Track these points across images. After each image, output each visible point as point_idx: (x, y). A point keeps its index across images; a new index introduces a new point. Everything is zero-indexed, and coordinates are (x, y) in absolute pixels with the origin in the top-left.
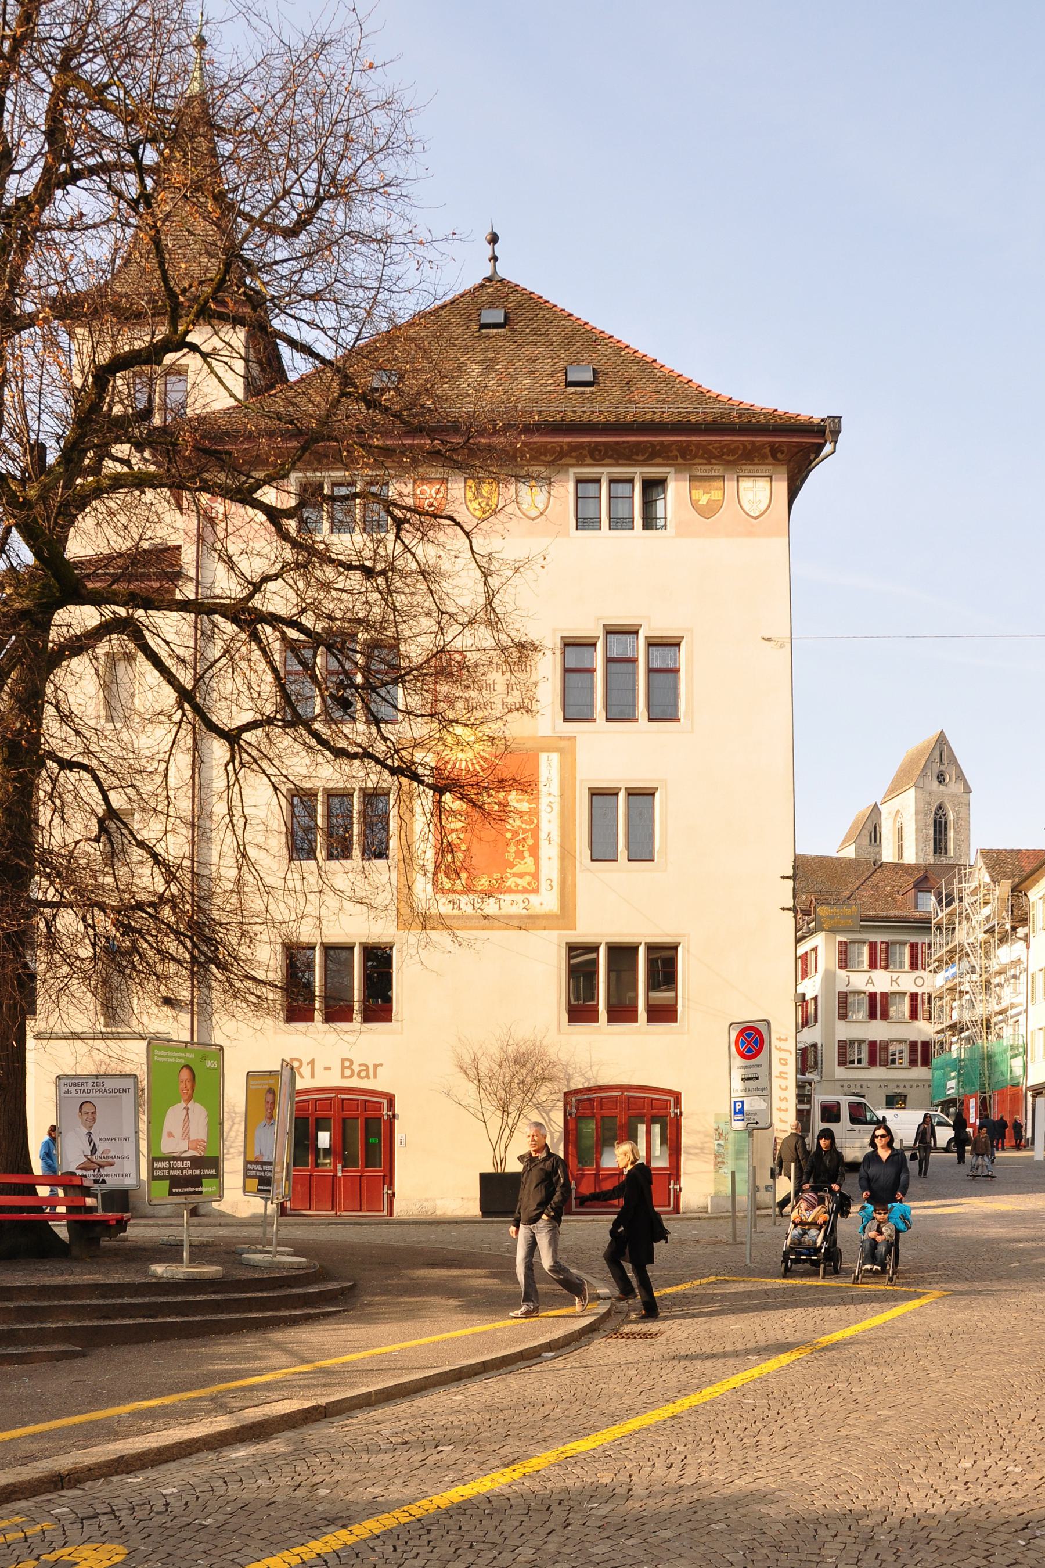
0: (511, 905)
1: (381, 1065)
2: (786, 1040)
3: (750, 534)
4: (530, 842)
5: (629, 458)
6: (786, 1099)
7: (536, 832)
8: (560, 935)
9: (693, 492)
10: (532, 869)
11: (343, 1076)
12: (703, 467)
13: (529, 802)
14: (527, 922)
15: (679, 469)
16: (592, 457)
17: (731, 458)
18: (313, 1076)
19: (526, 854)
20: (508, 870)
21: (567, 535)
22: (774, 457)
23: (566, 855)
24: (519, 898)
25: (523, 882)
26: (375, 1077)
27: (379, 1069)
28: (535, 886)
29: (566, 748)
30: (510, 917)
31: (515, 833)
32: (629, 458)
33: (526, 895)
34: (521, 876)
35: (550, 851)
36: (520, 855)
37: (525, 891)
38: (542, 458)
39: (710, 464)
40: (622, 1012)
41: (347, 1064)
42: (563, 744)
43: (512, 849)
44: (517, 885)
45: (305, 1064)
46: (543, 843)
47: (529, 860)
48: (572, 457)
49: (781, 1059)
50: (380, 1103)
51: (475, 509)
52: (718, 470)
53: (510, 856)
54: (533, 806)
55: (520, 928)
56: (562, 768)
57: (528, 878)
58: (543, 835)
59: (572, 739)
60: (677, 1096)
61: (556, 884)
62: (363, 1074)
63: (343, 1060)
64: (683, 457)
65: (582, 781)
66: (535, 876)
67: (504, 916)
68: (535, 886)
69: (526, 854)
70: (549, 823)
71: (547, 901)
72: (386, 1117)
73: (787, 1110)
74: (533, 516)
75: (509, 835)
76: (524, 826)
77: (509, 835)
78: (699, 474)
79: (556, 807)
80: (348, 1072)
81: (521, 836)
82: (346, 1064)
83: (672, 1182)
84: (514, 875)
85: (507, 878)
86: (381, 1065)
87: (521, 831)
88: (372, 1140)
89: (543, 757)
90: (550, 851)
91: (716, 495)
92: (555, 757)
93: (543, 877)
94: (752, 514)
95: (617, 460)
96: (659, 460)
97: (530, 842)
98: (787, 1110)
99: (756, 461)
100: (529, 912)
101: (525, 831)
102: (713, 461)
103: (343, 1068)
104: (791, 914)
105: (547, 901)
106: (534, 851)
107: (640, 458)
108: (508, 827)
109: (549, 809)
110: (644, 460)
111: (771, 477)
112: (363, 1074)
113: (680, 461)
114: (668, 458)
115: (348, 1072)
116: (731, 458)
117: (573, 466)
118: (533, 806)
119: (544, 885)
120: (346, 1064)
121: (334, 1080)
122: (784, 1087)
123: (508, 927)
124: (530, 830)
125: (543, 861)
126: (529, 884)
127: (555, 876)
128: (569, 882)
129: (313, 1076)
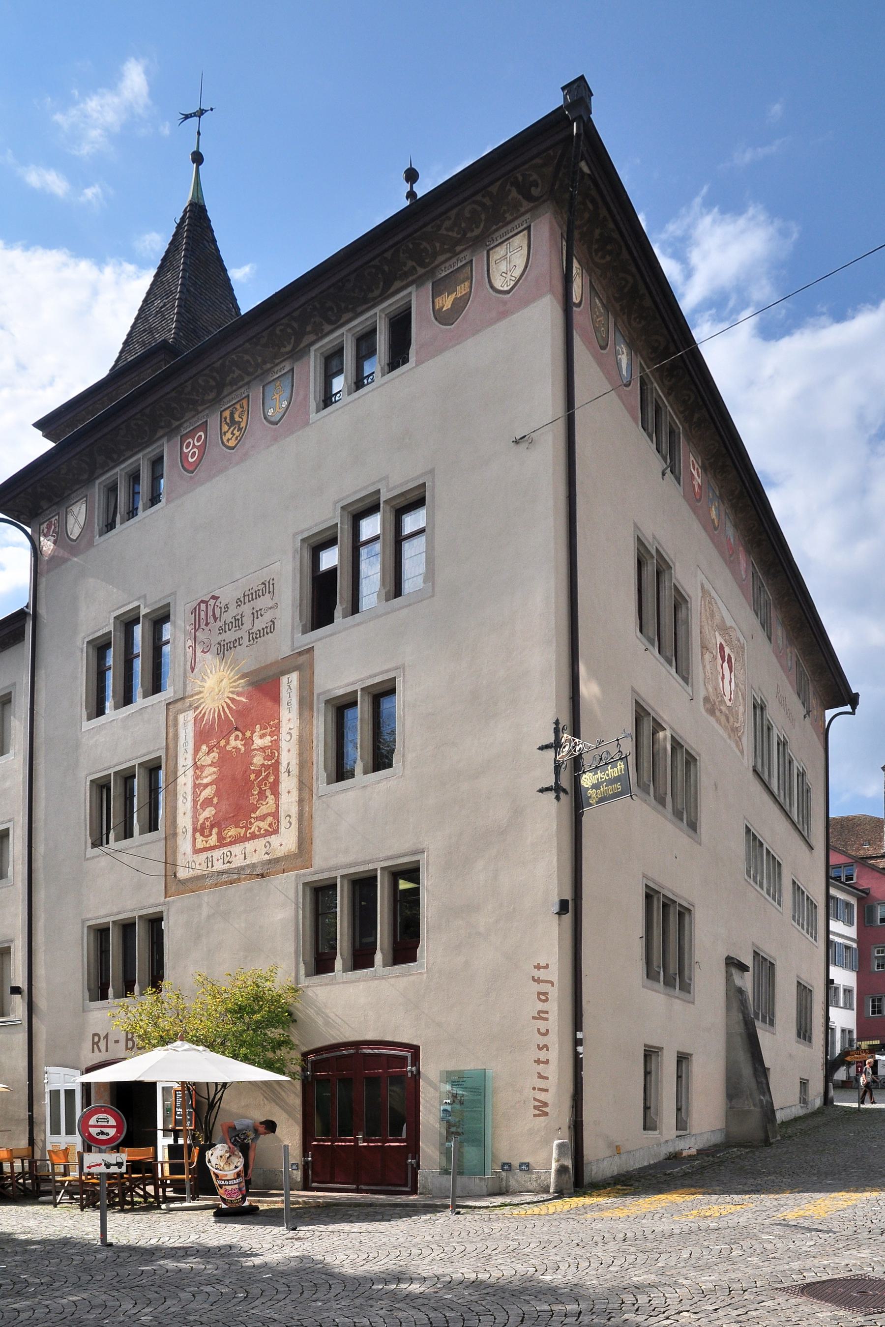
2: (547, 967)
3: (503, 315)
4: (271, 779)
6: (546, 1046)
9: (436, 300)
11: (127, 1049)
12: (447, 264)
15: (419, 282)
17: (477, 232)
19: (268, 793)
20: (253, 815)
21: (307, 423)
22: (529, 198)
23: (304, 785)
25: (264, 825)
29: (302, 662)
30: (254, 866)
31: (258, 773)
32: (365, 300)
35: (288, 784)
36: (262, 795)
37: (268, 833)
44: (260, 829)
46: (283, 776)
47: (271, 799)
48: (310, 333)
49: (539, 993)
51: (228, 440)
53: (253, 800)
54: (275, 737)
56: (301, 687)
57: (270, 819)
58: (283, 768)
60: (415, 1050)
61: (294, 820)
64: (422, 264)
65: (319, 695)
66: (275, 815)
67: (247, 865)
68: (275, 826)
69: (268, 793)
70: (288, 756)
73: (547, 1062)
75: (253, 777)
76: (266, 763)
77: (253, 777)
78: (443, 274)
79: (295, 734)
80: (130, 1044)
83: (410, 1155)
84: (257, 819)
89: (284, 680)
90: (288, 784)
91: (461, 290)
92: (294, 677)
93: (282, 815)
94: (506, 288)
96: (398, 284)
97: (271, 779)
98: (547, 1062)
99: (509, 217)
101: (267, 767)
102: (458, 248)
103: (127, 1040)
104: (552, 795)
105: (286, 841)
111: (528, 228)
113: (421, 271)
114: (406, 275)
115: (130, 1044)
116: (477, 232)
117: (313, 343)
118: (275, 737)
119: (284, 823)
122: (543, 1031)
123: (251, 876)
124: (270, 766)
126: (270, 825)
127: (294, 810)
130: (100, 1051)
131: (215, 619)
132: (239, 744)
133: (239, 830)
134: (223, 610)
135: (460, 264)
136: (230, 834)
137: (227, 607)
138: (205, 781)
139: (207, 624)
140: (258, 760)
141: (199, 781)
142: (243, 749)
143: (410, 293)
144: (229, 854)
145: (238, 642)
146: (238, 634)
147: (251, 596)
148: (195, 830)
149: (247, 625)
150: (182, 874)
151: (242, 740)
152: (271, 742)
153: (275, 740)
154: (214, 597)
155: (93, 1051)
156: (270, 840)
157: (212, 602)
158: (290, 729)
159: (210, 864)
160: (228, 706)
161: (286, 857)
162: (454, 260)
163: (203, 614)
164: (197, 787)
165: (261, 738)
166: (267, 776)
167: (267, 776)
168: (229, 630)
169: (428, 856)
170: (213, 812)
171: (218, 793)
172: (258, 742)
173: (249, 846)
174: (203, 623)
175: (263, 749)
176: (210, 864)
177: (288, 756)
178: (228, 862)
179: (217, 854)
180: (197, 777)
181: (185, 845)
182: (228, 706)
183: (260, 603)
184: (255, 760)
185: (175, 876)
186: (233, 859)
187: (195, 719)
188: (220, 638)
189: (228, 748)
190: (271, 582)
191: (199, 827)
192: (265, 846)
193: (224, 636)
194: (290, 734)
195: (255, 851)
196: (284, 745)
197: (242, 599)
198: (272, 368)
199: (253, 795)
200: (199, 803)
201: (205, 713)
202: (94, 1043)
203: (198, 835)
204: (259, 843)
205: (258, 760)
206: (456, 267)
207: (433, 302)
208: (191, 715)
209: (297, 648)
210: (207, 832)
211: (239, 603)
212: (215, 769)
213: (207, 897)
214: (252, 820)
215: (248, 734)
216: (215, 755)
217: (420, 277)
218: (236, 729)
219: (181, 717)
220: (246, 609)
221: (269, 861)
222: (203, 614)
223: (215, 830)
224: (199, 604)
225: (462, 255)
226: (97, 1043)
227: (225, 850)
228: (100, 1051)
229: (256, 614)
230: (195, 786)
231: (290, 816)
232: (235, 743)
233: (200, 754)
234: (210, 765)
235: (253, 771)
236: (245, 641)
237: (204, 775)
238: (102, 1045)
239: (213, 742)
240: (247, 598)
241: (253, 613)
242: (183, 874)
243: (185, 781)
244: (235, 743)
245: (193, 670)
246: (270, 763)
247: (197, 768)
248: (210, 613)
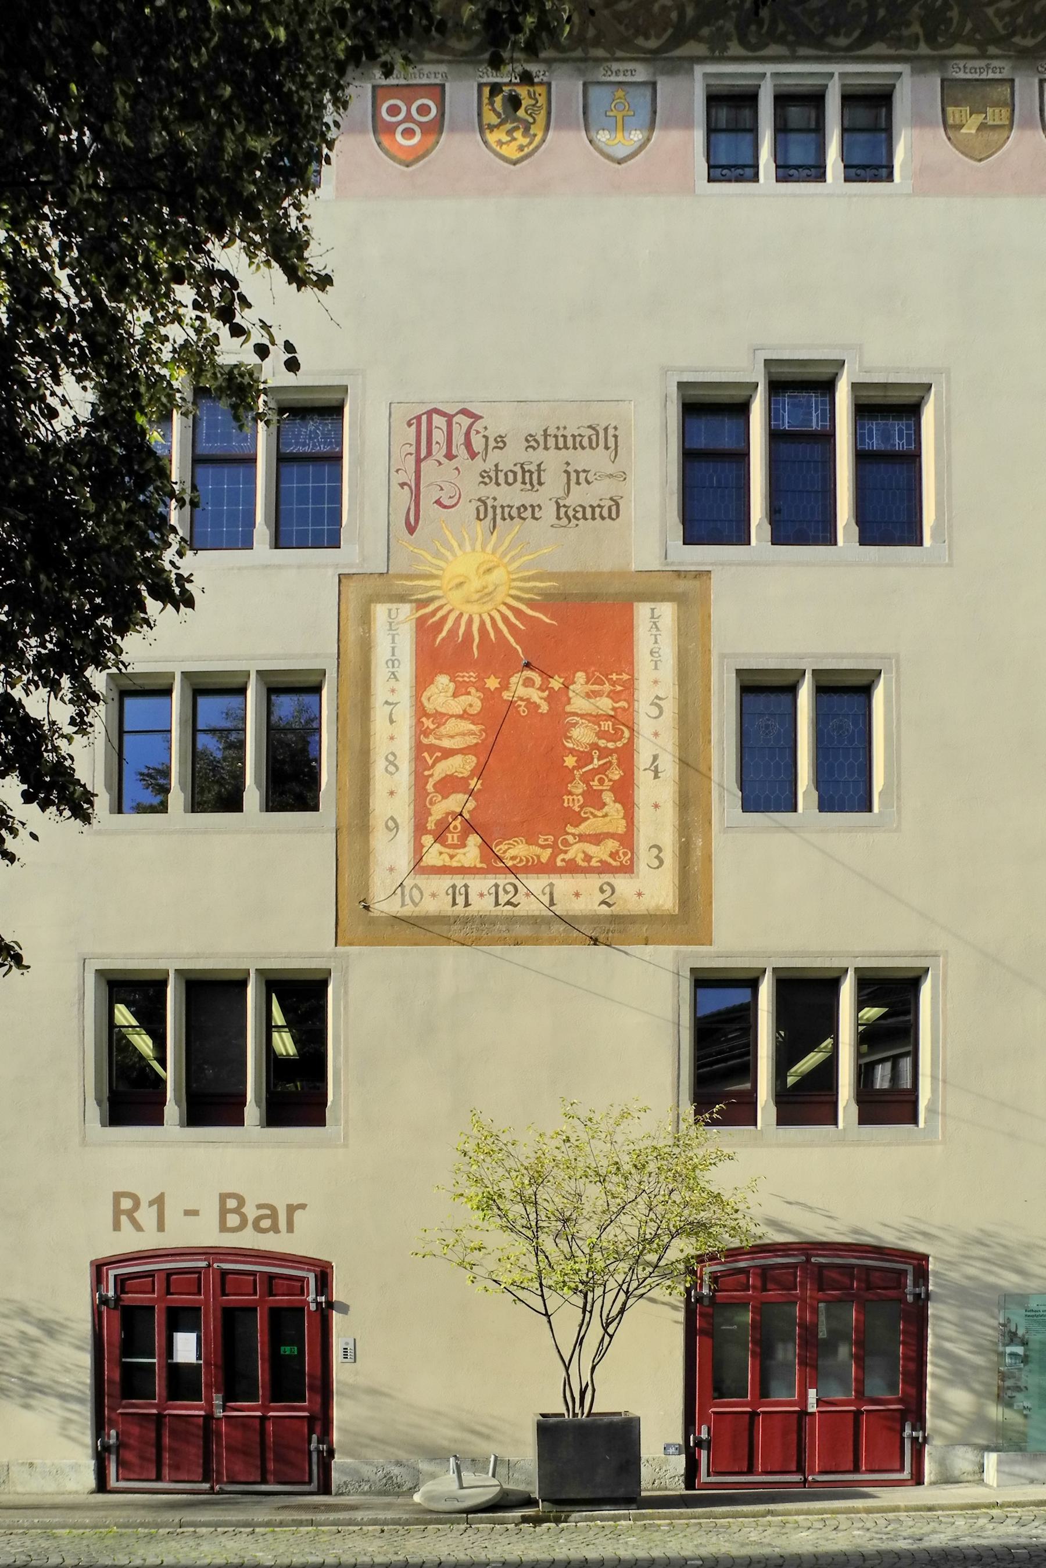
0: (577, 894)
1: (303, 1206)
4: (616, 774)
5: (818, 42)
7: (627, 756)
8: (677, 953)
9: (950, 110)
10: (621, 827)
11: (223, 1228)
12: (970, 64)
13: (614, 696)
14: (607, 931)
15: (920, 65)
16: (743, 42)
18: (161, 1227)
19: (608, 797)
20: (570, 829)
24: (594, 881)
25: (600, 853)
26: (290, 1228)
27: (298, 1215)
28: (625, 860)
29: (688, 593)
31: (584, 758)
33: (607, 878)
34: (597, 839)
35: (656, 794)
36: (594, 799)
37: (605, 868)
38: (640, 41)
39: (983, 56)
40: (806, 1102)
41: (232, 1204)
42: (681, 585)
43: (578, 788)
44: (588, 858)
45: (144, 1204)
46: (643, 779)
47: (614, 809)
50: (301, 1279)
52: (1000, 68)
53: (574, 801)
55: (595, 941)
57: (611, 845)
58: (643, 758)
59: (703, 575)
62: (266, 1224)
63: (223, 1198)
65: (723, 656)
66: (627, 839)
68: (625, 860)
69: (608, 797)
70: (655, 739)
71: (652, 888)
72: (313, 1307)
74: (621, 153)
75: (570, 761)
76: (602, 743)
78: (961, 75)
79: (670, 707)
80: (233, 1220)
81: (596, 763)
82: (230, 1204)
84: (582, 838)
85: (566, 843)
86: (303, 1206)
87: (596, 754)
88: (286, 1350)
89: (642, 611)
90: (656, 794)
92: (667, 611)
93: (642, 842)
95: (792, 46)
100: (615, 910)
101: (604, 753)
103: (224, 1212)
105: (652, 888)
106: (625, 791)
107: (843, 41)
108: (570, 745)
109: (655, 711)
110: (849, 48)
112: (266, 1224)
115: (233, 1220)
119: (644, 857)
120: (230, 1204)
121: (205, 1234)
125: (643, 814)
127: (668, 839)
128: (698, 853)
129: (161, 1227)
130: (138, 1228)
131: (473, 455)
132: (535, 695)
133: (538, 850)
134: (492, 444)
135: (991, 76)
136: (512, 852)
137: (501, 442)
138: (446, 743)
139: (450, 456)
140: (582, 735)
141: (431, 740)
142: (544, 708)
143: (899, 75)
144: (510, 888)
145: (528, 512)
146: (529, 498)
147: (563, 441)
148: (420, 829)
149: (553, 485)
150: (385, 905)
151: (541, 689)
152: (614, 709)
153: (624, 709)
154: (464, 412)
155: (117, 1226)
156: (612, 881)
157: (466, 421)
158: (657, 697)
159: (460, 900)
160: (505, 619)
161: (651, 918)
162: (982, 63)
163: (439, 436)
164: (424, 753)
165: (588, 695)
166: (604, 769)
167: (604, 769)
168: (510, 484)
169: (945, 965)
170: (471, 805)
171: (480, 772)
172: (579, 704)
173: (564, 884)
174: (439, 452)
175: (596, 718)
176: (460, 900)
177: (655, 739)
178: (508, 903)
179: (480, 885)
180: (420, 731)
181: (391, 852)
182: (505, 619)
183: (582, 459)
184: (575, 733)
185: (367, 908)
186: (519, 898)
187: (421, 622)
188: (484, 492)
189: (506, 695)
190: (611, 432)
191: (431, 826)
192: (602, 891)
193: (491, 490)
194: (660, 707)
195: (577, 895)
196: (645, 724)
197: (541, 440)
198: (606, 60)
199: (570, 793)
200: (431, 783)
201: (444, 619)
202: (117, 1212)
203: (427, 840)
204: (590, 884)
205: (582, 735)
206: (984, 76)
207: (943, 110)
208: (405, 610)
209: (672, 564)
210: (452, 838)
211: (531, 442)
212: (473, 727)
213: (450, 961)
214: (570, 838)
215: (556, 684)
216: (473, 701)
217: (918, 58)
218: (528, 665)
219: (380, 611)
220: (552, 460)
221: (615, 919)
222: (439, 436)
223: (474, 840)
224: (429, 414)
225: (996, 63)
226: (130, 1214)
227: (503, 880)
228: (138, 1228)
229: (573, 477)
230: (419, 749)
231: (660, 850)
232: (525, 690)
233: (432, 690)
234: (460, 717)
235: (572, 752)
236: (549, 512)
237: (443, 730)
238: (147, 1216)
239: (470, 676)
240: (551, 442)
241: (566, 471)
242: (385, 905)
243: (392, 734)
244: (525, 690)
245: (411, 529)
246: (611, 745)
247: (428, 716)
248: (458, 438)
